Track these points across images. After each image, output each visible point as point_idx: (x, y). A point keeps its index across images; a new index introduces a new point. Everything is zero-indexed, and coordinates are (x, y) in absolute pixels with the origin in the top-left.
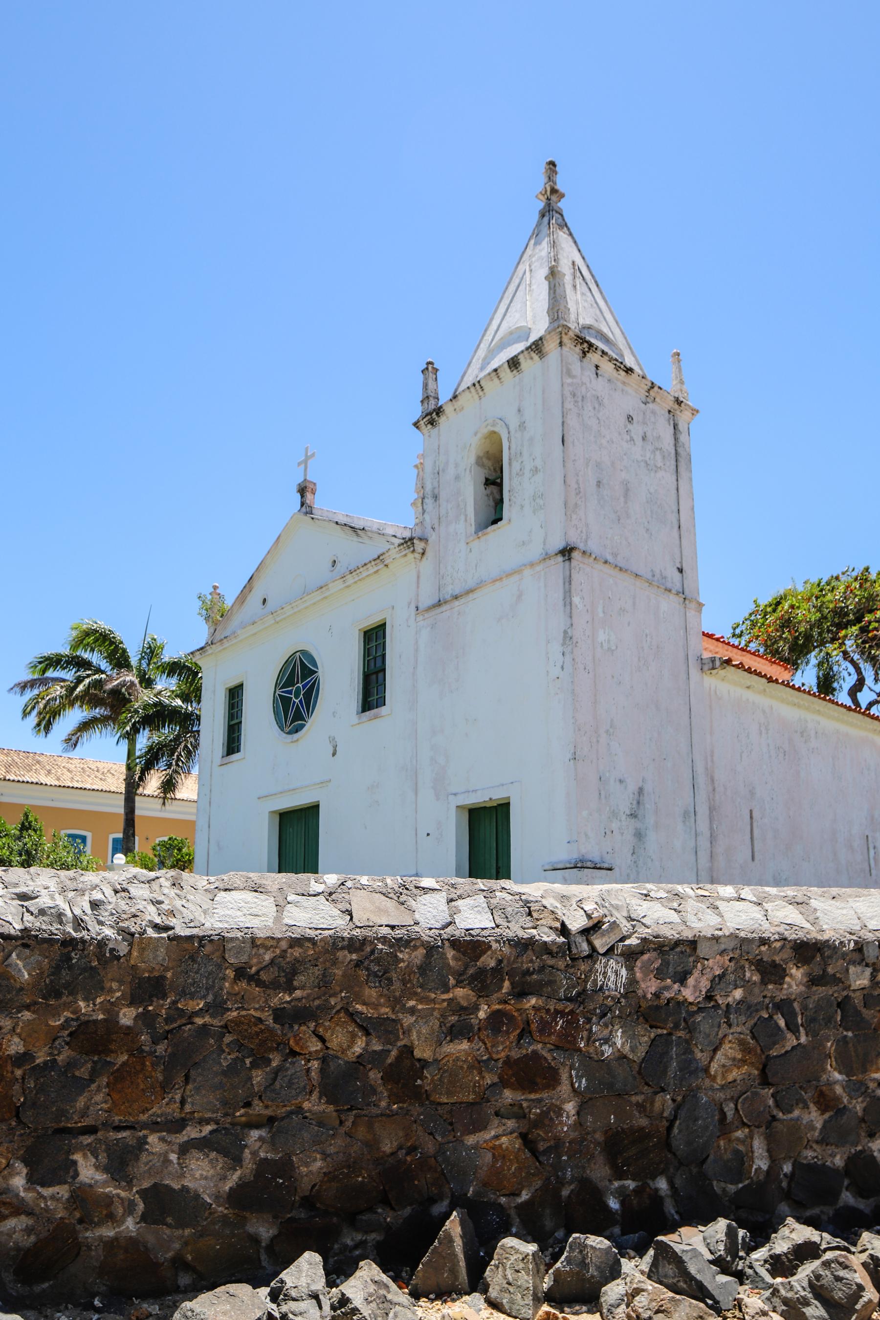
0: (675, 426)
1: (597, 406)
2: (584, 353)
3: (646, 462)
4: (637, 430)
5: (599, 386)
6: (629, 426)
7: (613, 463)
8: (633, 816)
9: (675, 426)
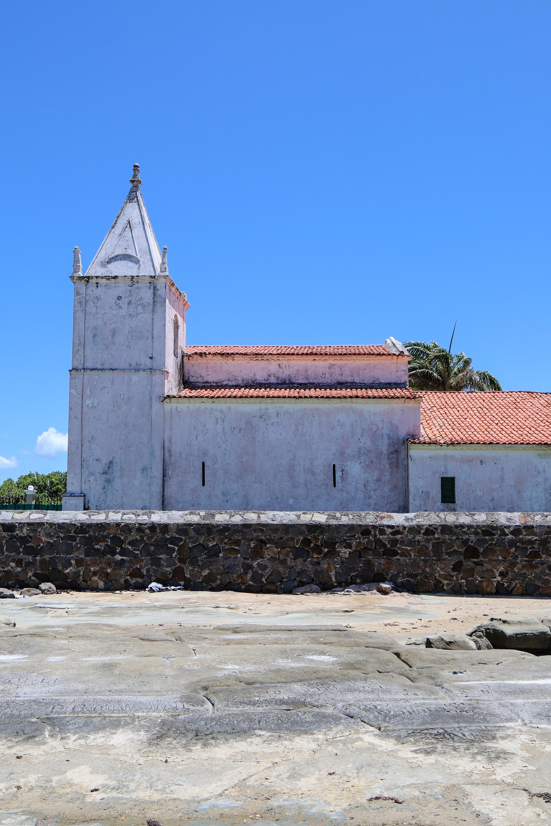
0: (155, 288)
1: (96, 301)
2: (88, 282)
3: (130, 315)
4: (125, 301)
5: (99, 292)
6: (118, 302)
7: (105, 324)
9: (155, 288)
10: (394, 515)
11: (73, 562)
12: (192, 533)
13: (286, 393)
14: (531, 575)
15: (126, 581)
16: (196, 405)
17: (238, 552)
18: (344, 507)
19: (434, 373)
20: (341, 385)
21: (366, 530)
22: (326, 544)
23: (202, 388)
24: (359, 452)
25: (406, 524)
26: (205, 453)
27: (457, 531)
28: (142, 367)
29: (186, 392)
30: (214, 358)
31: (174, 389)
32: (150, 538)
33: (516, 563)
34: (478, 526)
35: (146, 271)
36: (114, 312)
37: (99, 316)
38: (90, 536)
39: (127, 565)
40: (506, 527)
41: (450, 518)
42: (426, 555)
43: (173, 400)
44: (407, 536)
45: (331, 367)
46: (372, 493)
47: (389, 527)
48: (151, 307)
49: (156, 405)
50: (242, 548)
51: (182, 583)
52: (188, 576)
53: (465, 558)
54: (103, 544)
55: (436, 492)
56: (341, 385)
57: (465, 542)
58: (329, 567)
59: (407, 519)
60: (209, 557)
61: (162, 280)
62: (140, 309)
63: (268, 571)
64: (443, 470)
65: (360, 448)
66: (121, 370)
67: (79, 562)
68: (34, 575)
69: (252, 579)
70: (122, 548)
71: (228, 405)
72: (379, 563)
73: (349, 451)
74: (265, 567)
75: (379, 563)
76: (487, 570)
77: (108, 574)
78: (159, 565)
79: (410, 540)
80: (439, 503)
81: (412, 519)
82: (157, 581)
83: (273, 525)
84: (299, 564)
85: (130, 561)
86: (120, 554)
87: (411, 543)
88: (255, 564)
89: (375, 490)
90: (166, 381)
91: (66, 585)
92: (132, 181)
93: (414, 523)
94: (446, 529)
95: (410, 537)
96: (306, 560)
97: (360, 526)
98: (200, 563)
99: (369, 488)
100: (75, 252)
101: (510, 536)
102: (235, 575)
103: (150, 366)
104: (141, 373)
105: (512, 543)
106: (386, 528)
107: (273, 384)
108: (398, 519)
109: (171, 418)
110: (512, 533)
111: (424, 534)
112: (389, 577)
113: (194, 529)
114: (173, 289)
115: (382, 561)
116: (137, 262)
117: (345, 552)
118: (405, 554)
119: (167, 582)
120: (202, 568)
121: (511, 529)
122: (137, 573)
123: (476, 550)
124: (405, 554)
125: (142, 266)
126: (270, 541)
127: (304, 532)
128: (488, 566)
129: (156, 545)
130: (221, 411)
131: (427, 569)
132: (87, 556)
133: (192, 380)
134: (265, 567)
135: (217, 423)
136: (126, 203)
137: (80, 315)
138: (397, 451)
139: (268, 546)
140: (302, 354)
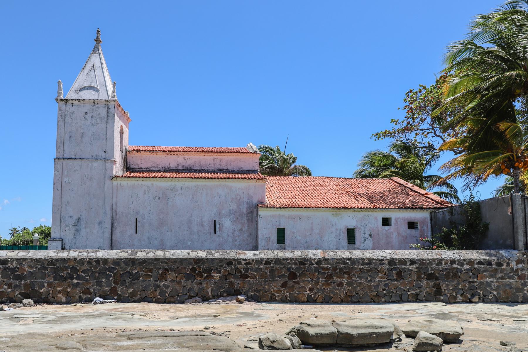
0: (108, 108)
4: (89, 116)
8: (75, 225)
9: (108, 108)
10: (247, 252)
11: (45, 284)
12: (123, 265)
13: (188, 175)
14: (327, 290)
15: (80, 297)
16: (132, 182)
17: (151, 276)
18: (220, 247)
19: (276, 166)
20: (220, 171)
21: (230, 262)
22: (205, 271)
24: (230, 212)
25: (254, 258)
26: (138, 213)
27: (284, 262)
28: (100, 158)
29: (128, 174)
30: (145, 153)
31: (120, 172)
32: (95, 268)
33: (319, 282)
34: (296, 259)
35: (103, 97)
36: (83, 122)
37: (74, 124)
38: (57, 267)
39: (81, 286)
40: (313, 259)
41: (280, 254)
42: (266, 277)
43: (118, 179)
44: (254, 265)
45: (214, 160)
46: (237, 238)
47: (243, 260)
48: (106, 119)
49: (108, 182)
50: (154, 274)
51: (116, 297)
52: (120, 293)
53: (289, 279)
54: (65, 272)
55: (274, 237)
56: (220, 171)
57: (289, 269)
58: (207, 286)
59: (254, 255)
60: (133, 280)
61: (113, 103)
62: (98, 120)
63: (170, 289)
64: (278, 224)
65: (230, 210)
66: (86, 159)
67: (50, 285)
68: (20, 294)
69: (160, 294)
70: (77, 275)
71: (152, 182)
72: (238, 283)
73: (223, 212)
74: (168, 286)
75: (238, 283)
76: (302, 287)
77: (68, 292)
78: (101, 286)
79: (256, 268)
80: (276, 244)
81: (257, 255)
82: (100, 296)
83: (173, 259)
84: (189, 284)
85: (83, 284)
86: (76, 279)
87: (257, 270)
88: (162, 284)
89: (239, 236)
90: (114, 166)
91: (41, 300)
92: (96, 41)
93: (259, 257)
94: (278, 261)
95: (256, 266)
96: (193, 282)
97: (226, 259)
98: (127, 284)
99: (235, 235)
100: (59, 83)
101: (315, 265)
102: (149, 292)
103: (104, 157)
104: (99, 161)
105: (316, 270)
106: (242, 261)
107: (180, 170)
108: (249, 255)
109: (117, 190)
110: (316, 263)
111: (265, 264)
112: (243, 292)
113: (124, 262)
114: (120, 109)
115: (240, 282)
116: (97, 91)
117: (217, 276)
118: (254, 277)
119: (105, 297)
120: (129, 287)
121: (316, 261)
122: (87, 291)
123: (295, 274)
124: (254, 277)
125: (101, 94)
126: (171, 269)
127: (192, 264)
128: (302, 284)
129: (100, 272)
130: (148, 186)
131: (266, 287)
132: (54, 280)
133: (132, 166)
134: (168, 286)
135: (145, 193)
136: (92, 54)
137: (61, 124)
138: (252, 212)
139: (170, 272)
140: (198, 152)
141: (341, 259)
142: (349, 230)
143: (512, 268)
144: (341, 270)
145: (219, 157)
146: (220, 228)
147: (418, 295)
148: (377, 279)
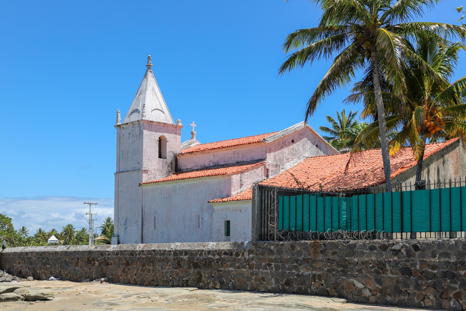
21: (102, 253)
23: (189, 172)
29: (174, 177)
47: (108, 252)
57: (126, 259)
133: (182, 168)
141: (149, 251)
142: (228, 221)
143: (245, 259)
144: (149, 259)
145: (236, 150)
146: (202, 222)
147: (188, 281)
148: (167, 267)
